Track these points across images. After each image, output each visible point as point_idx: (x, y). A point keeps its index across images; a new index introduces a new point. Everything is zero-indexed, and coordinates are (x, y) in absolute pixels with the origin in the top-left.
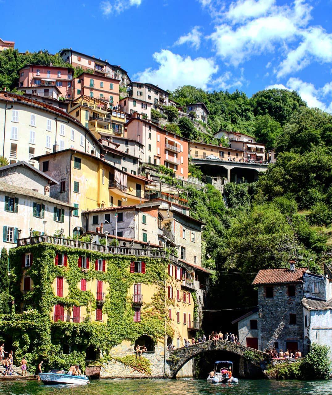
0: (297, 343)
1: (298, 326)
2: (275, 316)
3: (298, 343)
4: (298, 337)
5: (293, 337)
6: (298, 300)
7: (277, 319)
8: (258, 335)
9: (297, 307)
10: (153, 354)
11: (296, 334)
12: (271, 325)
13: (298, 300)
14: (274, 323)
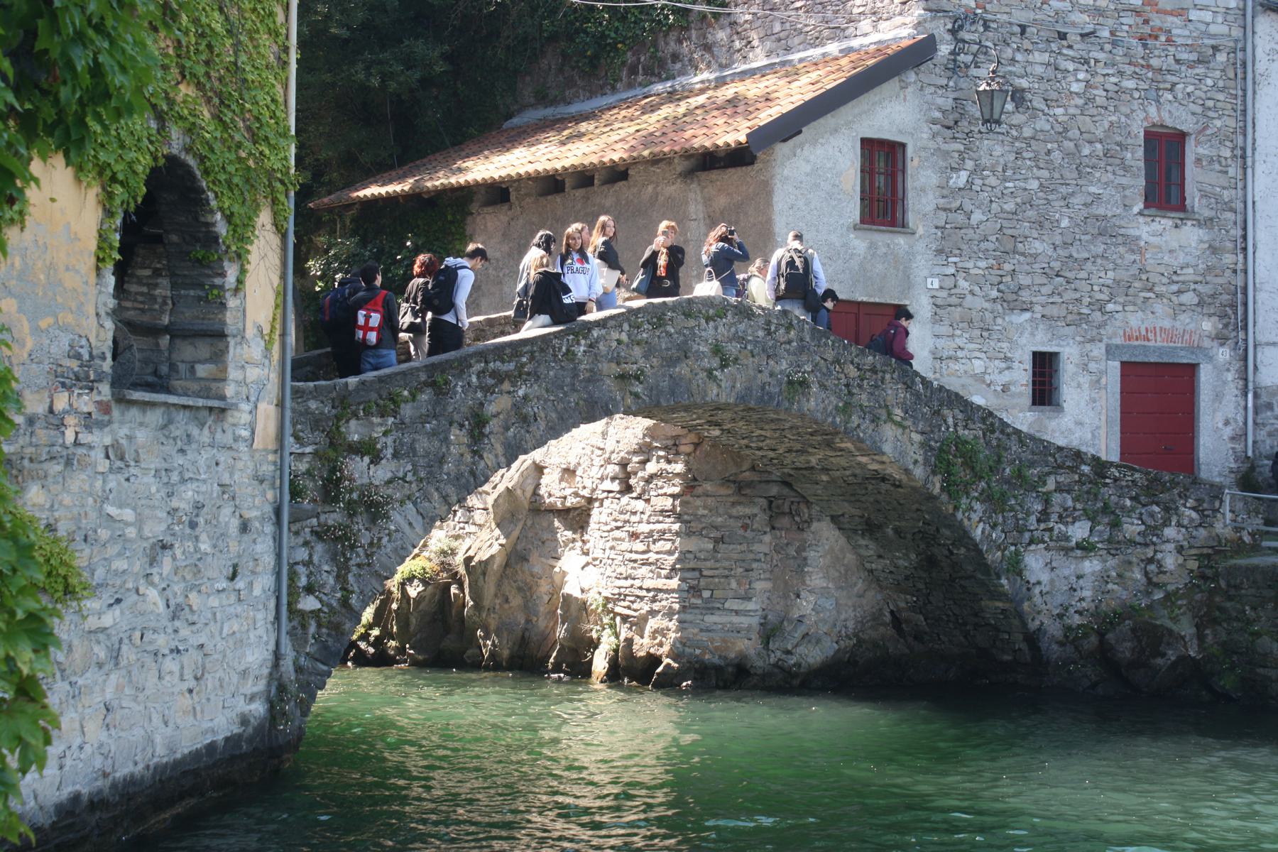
0: (1192, 369)
1: (1201, 233)
2: (1042, 124)
3: (1205, 376)
4: (1208, 325)
5: (1167, 324)
6: (1208, 16)
7: (1056, 155)
8: (907, 283)
9: (1200, 70)
11: (1189, 298)
12: (1010, 206)
13: (1208, 16)
14: (1034, 185)
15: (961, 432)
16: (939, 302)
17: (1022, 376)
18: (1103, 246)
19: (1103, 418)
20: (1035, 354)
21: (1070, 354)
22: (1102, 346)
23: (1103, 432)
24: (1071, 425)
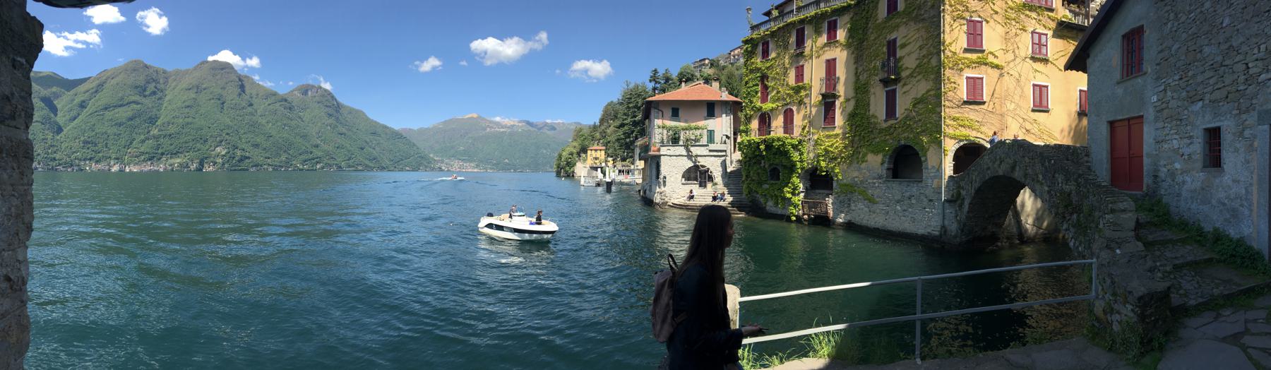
10: (920, 185)
15: (1064, 186)
16: (1158, 109)
17: (1197, 147)
18: (1256, 25)
19: (1255, 177)
20: (1206, 130)
21: (1228, 126)
22: (1255, 114)
23: (1255, 189)
24: (1230, 182)
